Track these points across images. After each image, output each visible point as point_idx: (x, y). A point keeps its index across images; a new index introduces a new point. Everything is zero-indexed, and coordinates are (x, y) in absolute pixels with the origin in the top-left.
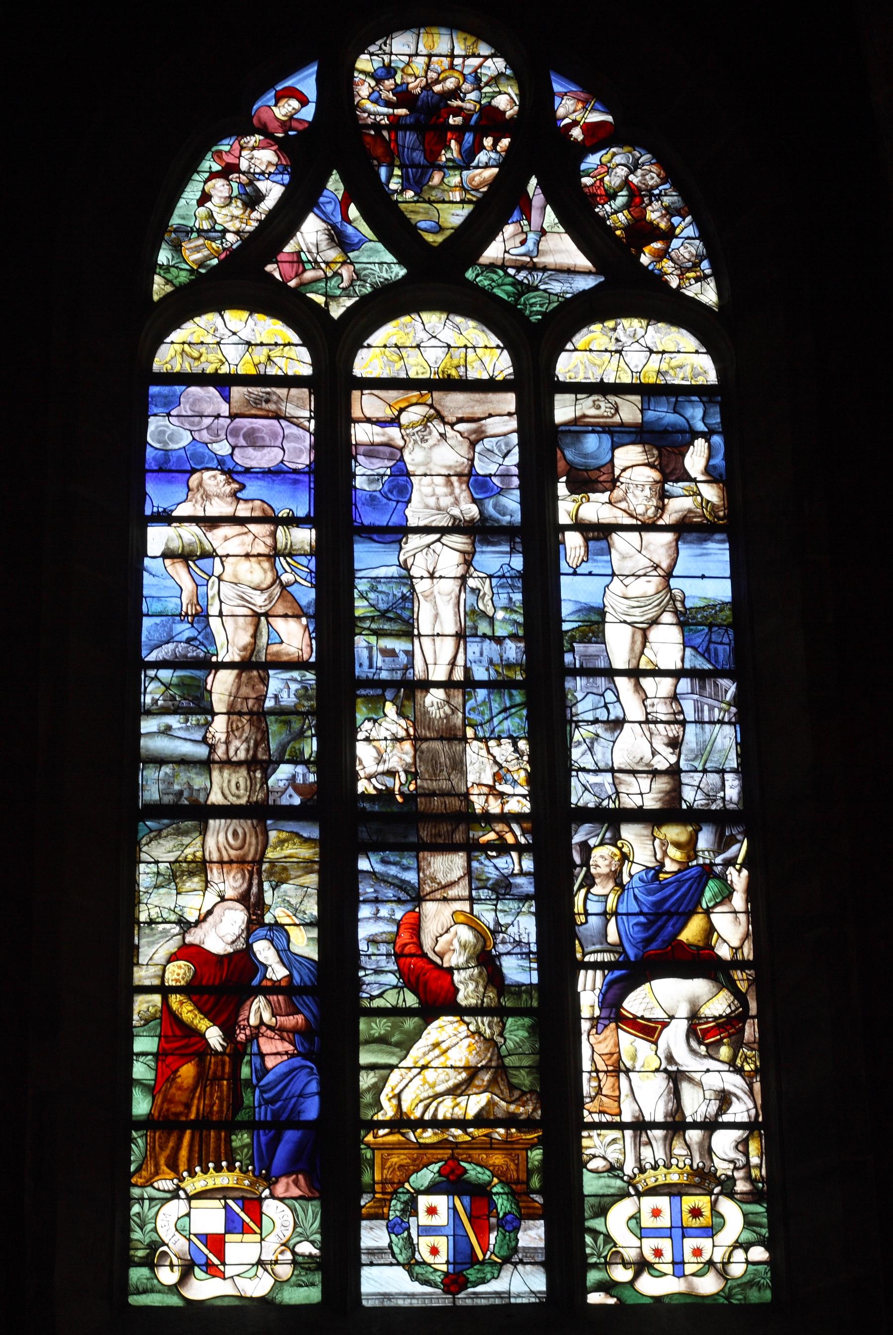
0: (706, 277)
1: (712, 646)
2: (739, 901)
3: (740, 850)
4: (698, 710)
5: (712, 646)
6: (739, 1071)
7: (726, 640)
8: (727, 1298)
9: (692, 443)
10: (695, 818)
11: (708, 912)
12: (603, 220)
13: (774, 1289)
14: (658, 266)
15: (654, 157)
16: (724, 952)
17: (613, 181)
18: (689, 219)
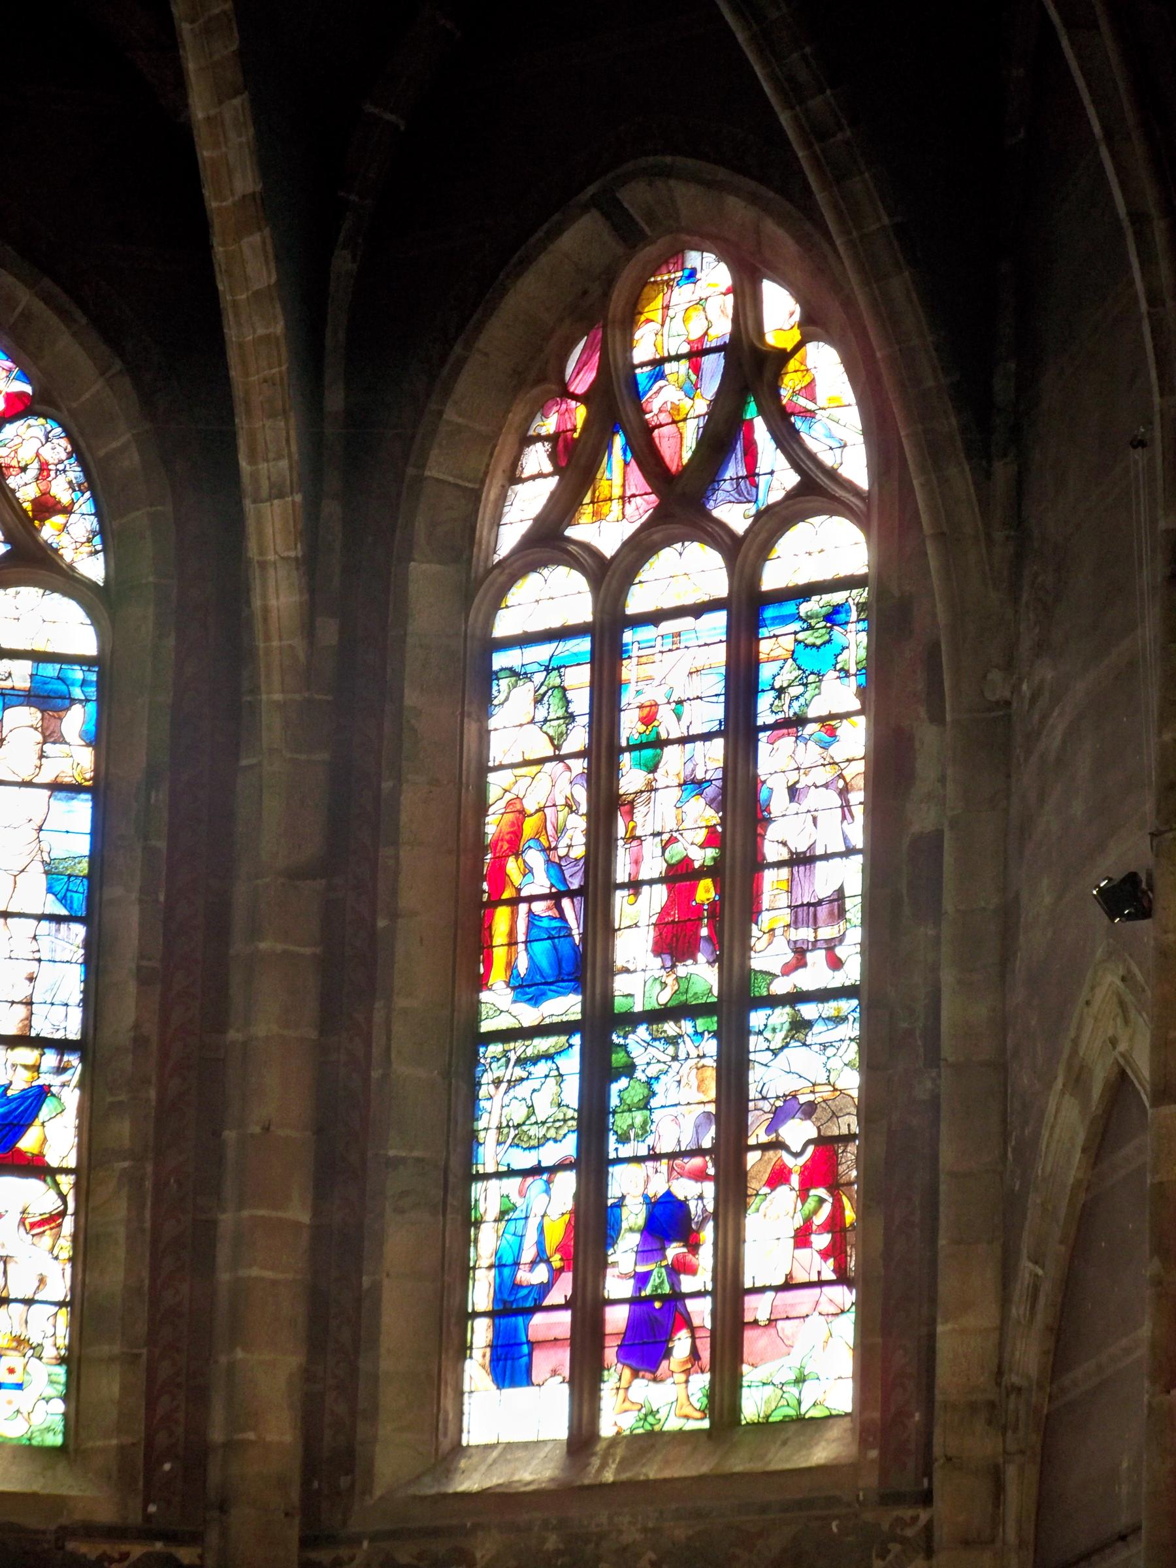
0: (97, 552)
1: (69, 894)
2: (70, 1119)
3: (74, 1075)
4: (53, 951)
5: (69, 894)
6: (56, 1258)
7: (81, 889)
8: (30, 1439)
9: (68, 709)
10: (41, 1043)
11: (43, 1124)
12: (13, 491)
13: (66, 1434)
14: (57, 539)
15: (64, 431)
16: (53, 1160)
17: (26, 454)
18: (88, 494)
